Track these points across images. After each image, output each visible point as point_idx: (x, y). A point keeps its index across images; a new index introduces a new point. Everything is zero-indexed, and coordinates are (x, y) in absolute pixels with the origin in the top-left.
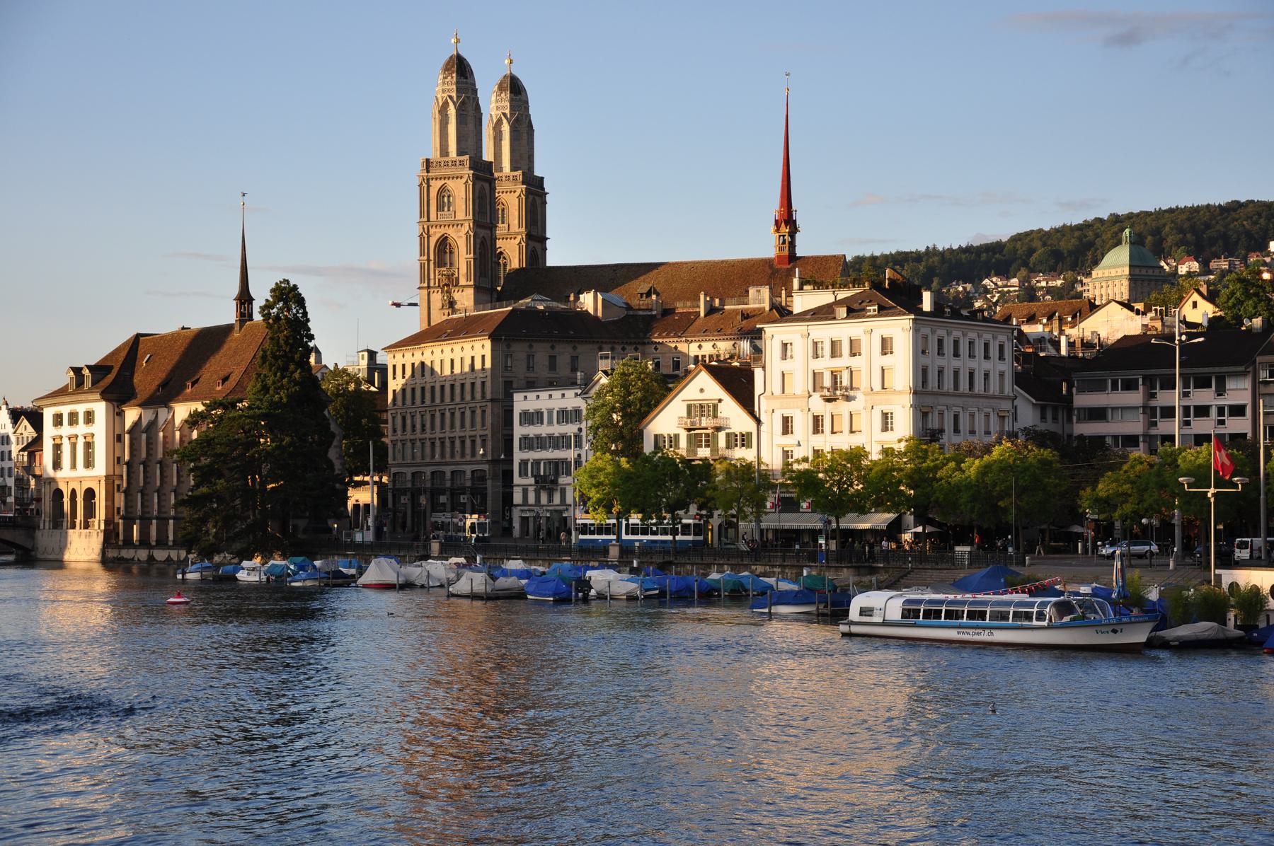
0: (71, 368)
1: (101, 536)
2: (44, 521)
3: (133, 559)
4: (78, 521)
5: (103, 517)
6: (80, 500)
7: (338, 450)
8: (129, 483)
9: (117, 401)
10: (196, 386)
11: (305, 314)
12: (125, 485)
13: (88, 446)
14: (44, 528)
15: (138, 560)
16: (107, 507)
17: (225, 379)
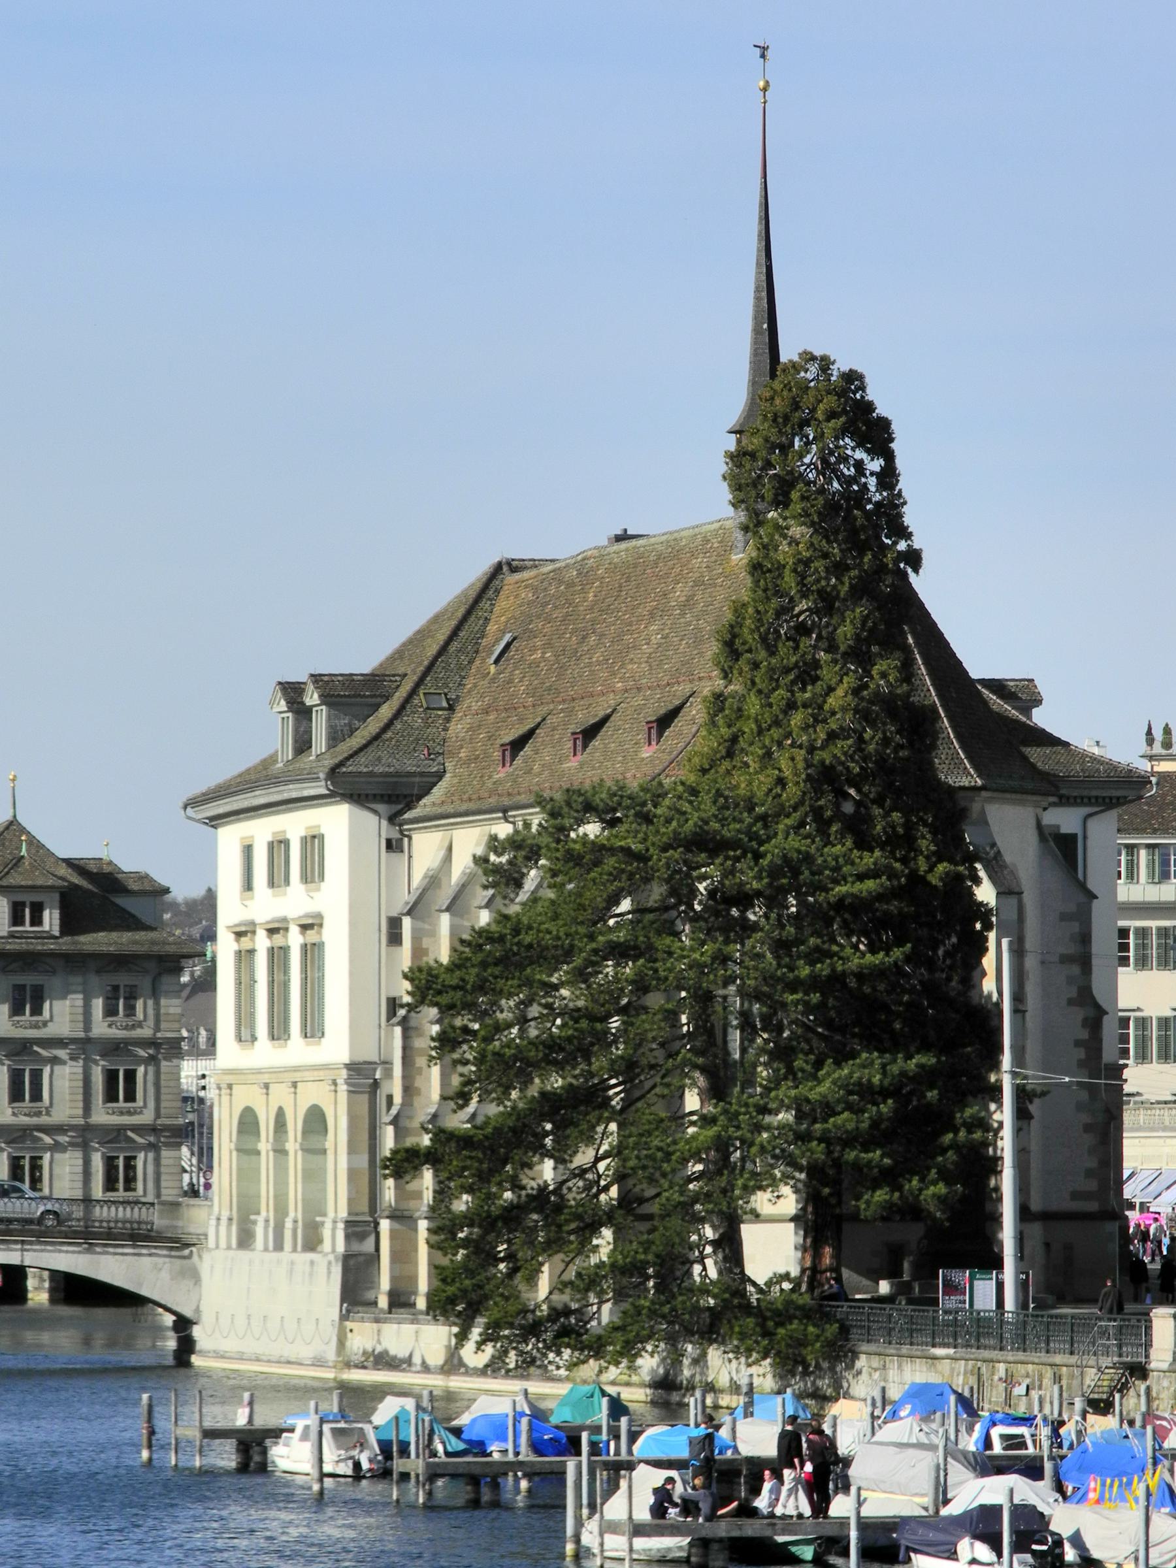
0: (280, 683)
1: (337, 1271)
2: (218, 1219)
3: (409, 1361)
4: (289, 1224)
5: (343, 1213)
6: (292, 1145)
7: (1076, 970)
8: (409, 1090)
9: (388, 799)
10: (596, 743)
11: (888, 477)
12: (398, 1099)
13: (313, 954)
14: (217, 1247)
15: (424, 1362)
16: (352, 1174)
17: (665, 722)
